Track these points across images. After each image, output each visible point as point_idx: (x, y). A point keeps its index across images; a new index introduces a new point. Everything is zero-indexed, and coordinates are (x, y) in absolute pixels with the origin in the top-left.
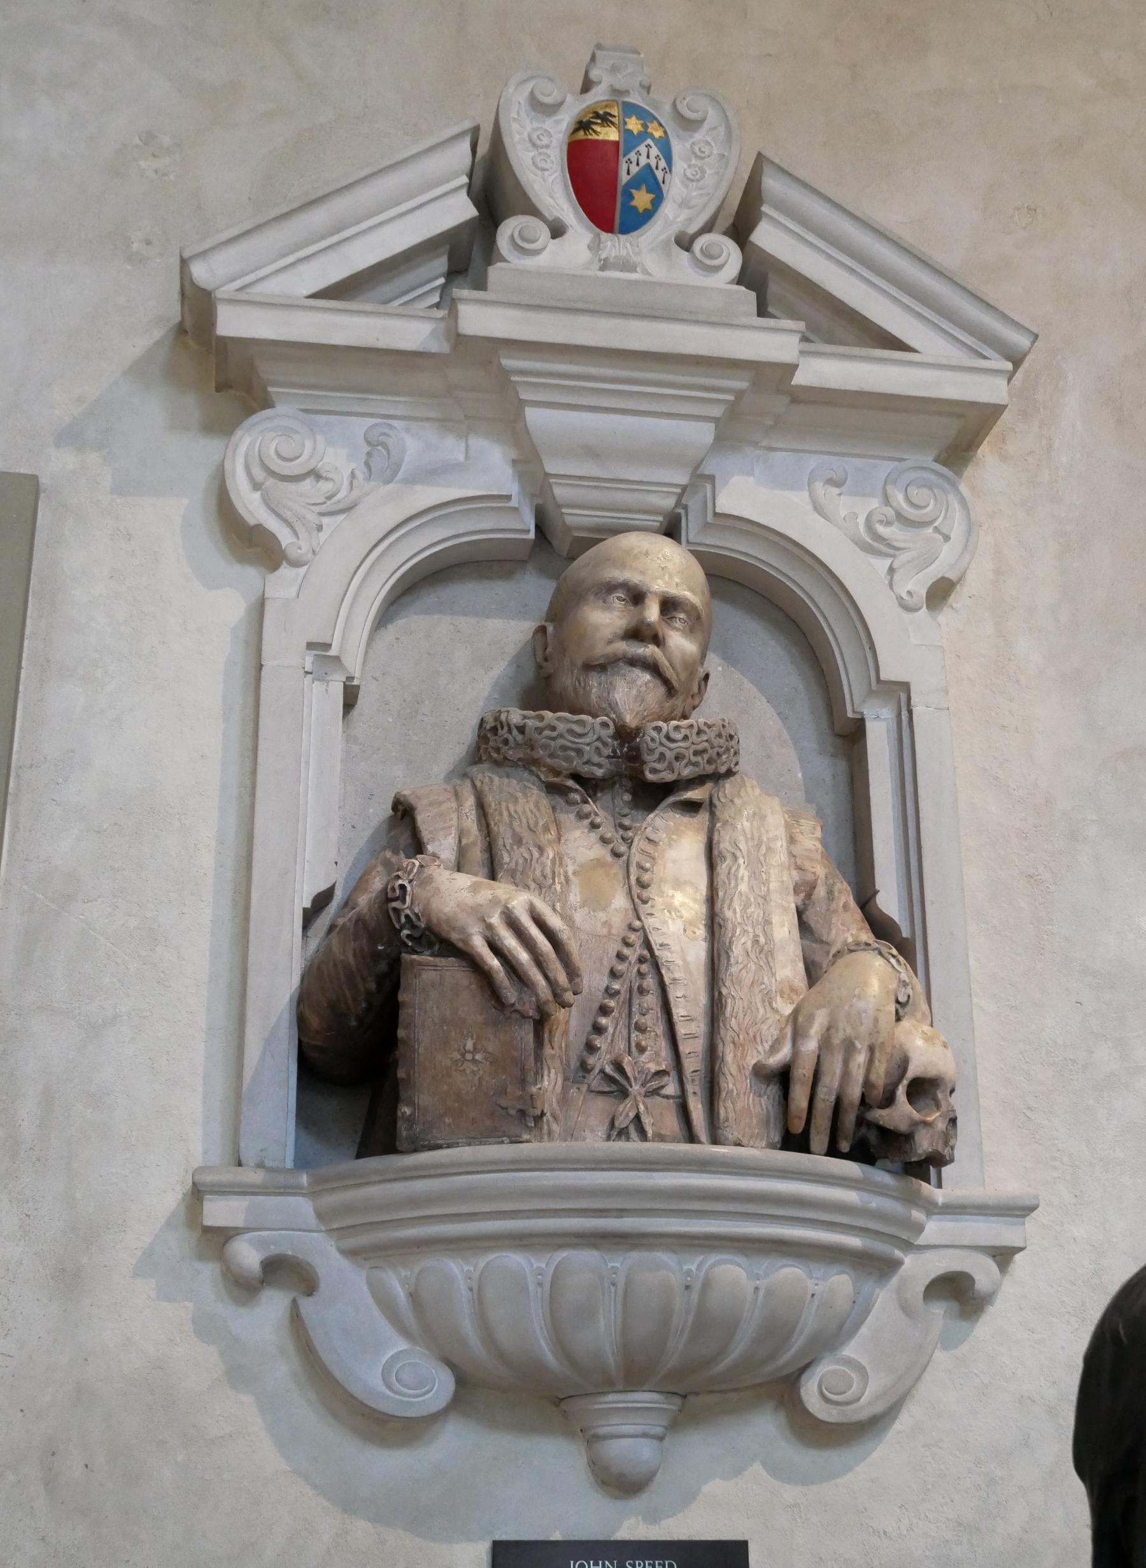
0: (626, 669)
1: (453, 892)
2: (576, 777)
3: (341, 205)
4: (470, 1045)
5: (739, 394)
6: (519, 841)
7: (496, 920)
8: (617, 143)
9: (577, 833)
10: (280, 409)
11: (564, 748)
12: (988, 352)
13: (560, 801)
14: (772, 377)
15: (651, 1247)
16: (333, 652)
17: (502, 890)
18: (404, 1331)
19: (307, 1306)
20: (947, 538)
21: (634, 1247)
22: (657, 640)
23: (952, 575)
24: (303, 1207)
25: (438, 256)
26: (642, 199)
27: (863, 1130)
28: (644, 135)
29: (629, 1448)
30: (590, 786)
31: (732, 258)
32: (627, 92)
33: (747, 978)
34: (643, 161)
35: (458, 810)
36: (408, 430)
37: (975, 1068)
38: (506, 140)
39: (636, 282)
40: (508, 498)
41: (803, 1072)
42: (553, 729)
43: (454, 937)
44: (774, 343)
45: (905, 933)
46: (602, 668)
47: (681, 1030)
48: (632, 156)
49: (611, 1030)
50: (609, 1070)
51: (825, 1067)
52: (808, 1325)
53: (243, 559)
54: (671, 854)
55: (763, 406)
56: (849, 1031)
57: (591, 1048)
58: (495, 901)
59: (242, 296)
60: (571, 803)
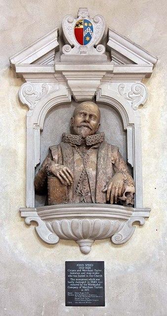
1: (55, 167)
2: (76, 145)
5: (104, 76)
10: (27, 82)
12: (149, 63)
16: (38, 124)
17: (62, 167)
18: (52, 232)
19: (37, 228)
22: (88, 122)
24: (36, 213)
26: (88, 39)
28: (88, 26)
29: (86, 248)
33: (101, 177)
38: (63, 30)
39: (86, 56)
41: (109, 192)
47: (91, 186)
53: (22, 108)
58: (60, 168)
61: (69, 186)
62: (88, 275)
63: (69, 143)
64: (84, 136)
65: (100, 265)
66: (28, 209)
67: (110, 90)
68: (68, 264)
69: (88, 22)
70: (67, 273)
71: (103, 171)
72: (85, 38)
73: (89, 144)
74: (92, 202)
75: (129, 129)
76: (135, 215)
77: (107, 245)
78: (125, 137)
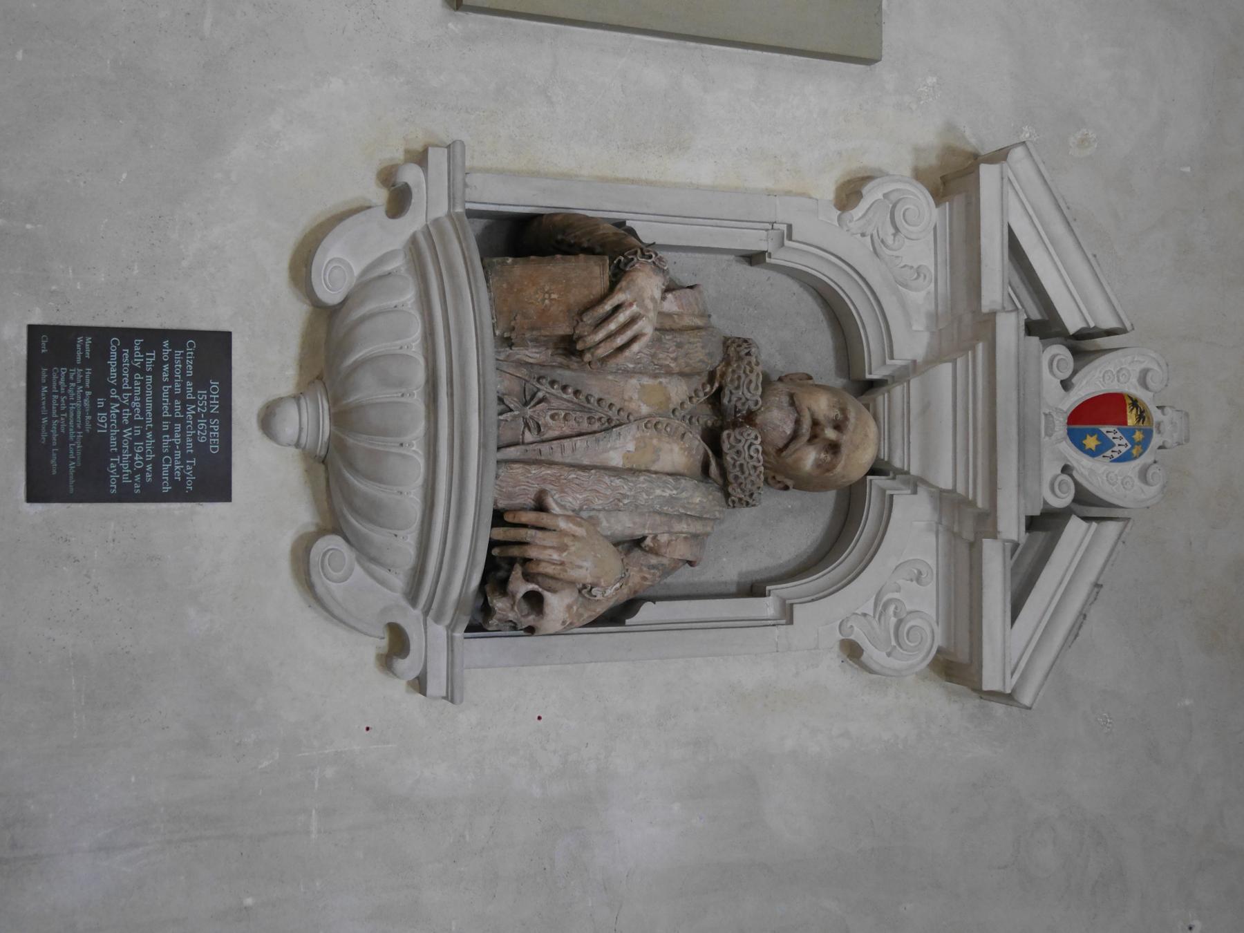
0: (793, 416)
2: (720, 389)
3: (1068, 242)
4: (553, 296)
5: (973, 503)
6: (679, 346)
7: (635, 308)
8: (1125, 423)
9: (685, 388)
11: (739, 378)
12: (1016, 676)
13: (705, 379)
14: (987, 521)
15: (428, 418)
16: (787, 243)
20: (889, 655)
21: (427, 407)
22: (813, 438)
23: (864, 658)
24: (441, 210)
25: (1040, 313)
26: (1091, 442)
27: (505, 565)
29: (291, 422)
30: (715, 399)
31: (1061, 500)
32: (1159, 432)
33: (601, 488)
34: (1116, 442)
35: (693, 315)
36: (929, 293)
37: (544, 664)
39: (1040, 435)
40: (892, 358)
41: (544, 519)
42: (751, 371)
43: (623, 283)
44: (1011, 525)
45: (628, 621)
46: (792, 403)
47: (566, 442)
48: (1119, 434)
49: (565, 396)
50: (540, 395)
51: (548, 533)
52: (378, 536)
54: (676, 448)
55: (965, 520)
56: (573, 549)
57: (552, 383)
58: (647, 310)
59: (1006, 180)
60: (704, 385)
61: (569, 347)
62: (171, 432)
63: (727, 361)
64: (759, 420)
65: (213, 482)
66: (459, 177)
67: (910, 535)
68: (224, 339)
69: (1145, 444)
70: (178, 337)
71: (625, 496)
72: (1092, 433)
73: (728, 439)
74: (499, 448)
75: (767, 606)
76: (432, 639)
77: (303, 516)
78: (733, 589)
